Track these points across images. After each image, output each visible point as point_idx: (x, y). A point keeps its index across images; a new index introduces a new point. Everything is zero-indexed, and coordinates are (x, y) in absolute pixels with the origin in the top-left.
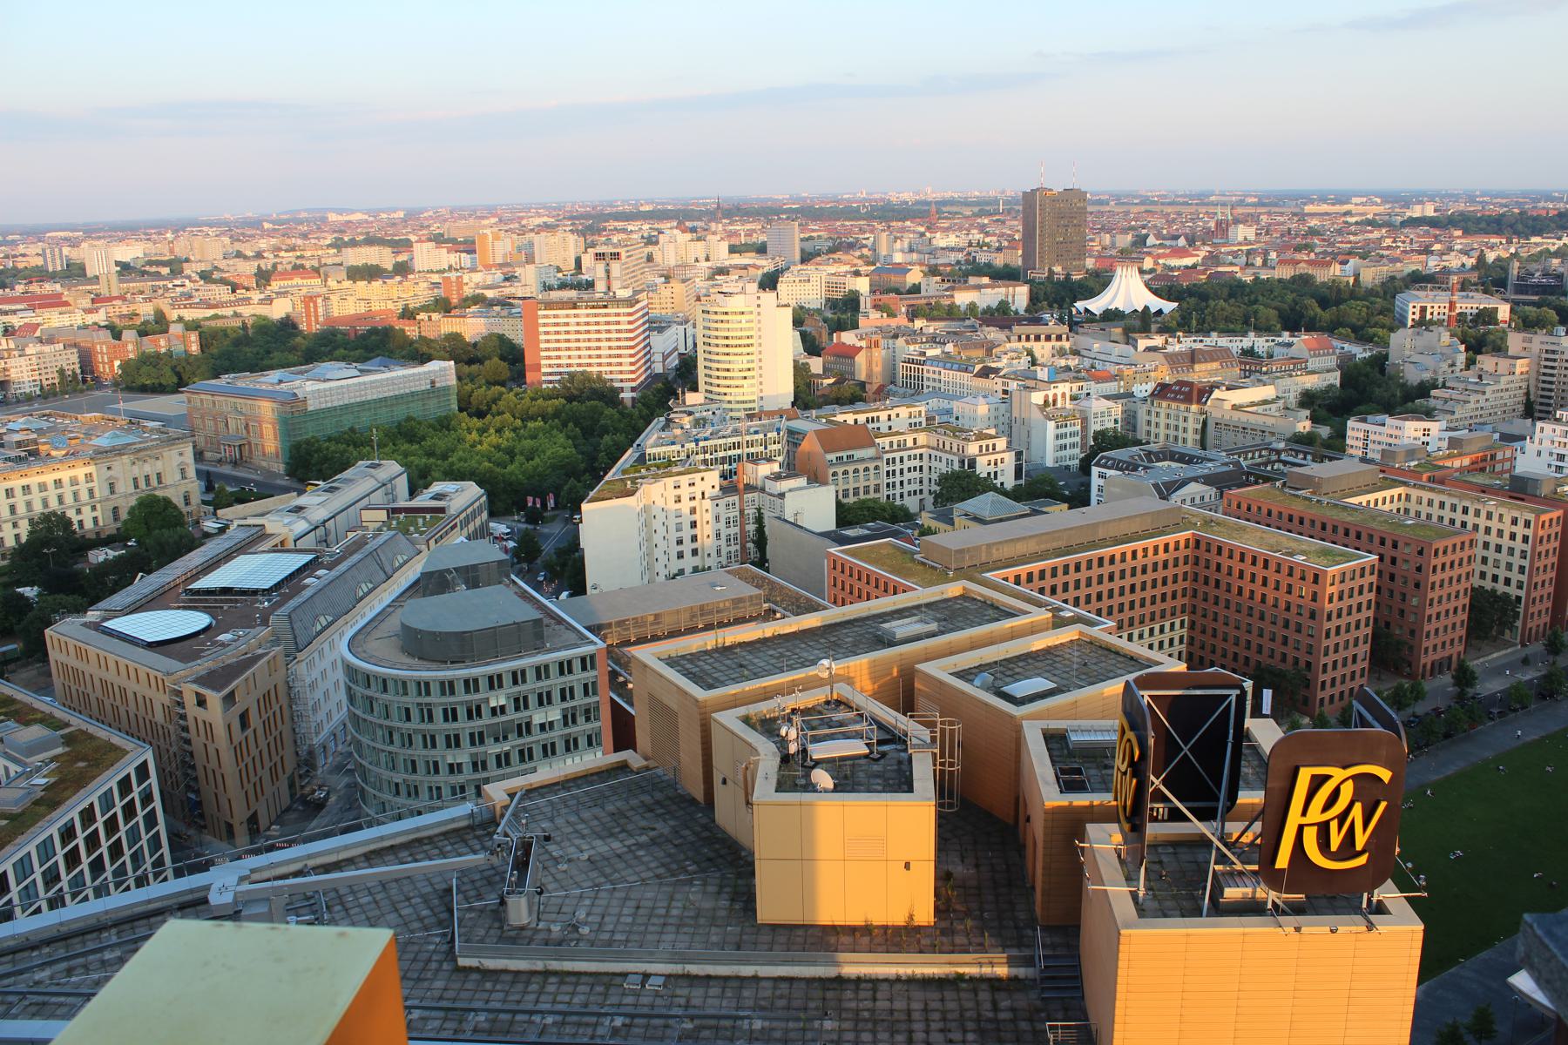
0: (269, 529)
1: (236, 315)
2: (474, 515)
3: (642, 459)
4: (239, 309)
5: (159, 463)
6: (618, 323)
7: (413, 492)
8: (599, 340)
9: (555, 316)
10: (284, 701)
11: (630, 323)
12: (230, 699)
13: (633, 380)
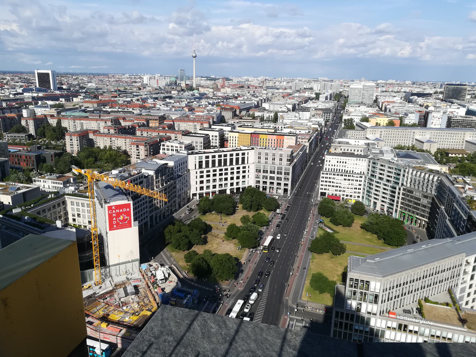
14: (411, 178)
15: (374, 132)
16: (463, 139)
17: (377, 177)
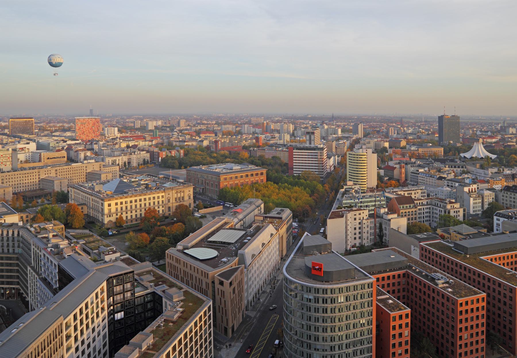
16: (39, 178)
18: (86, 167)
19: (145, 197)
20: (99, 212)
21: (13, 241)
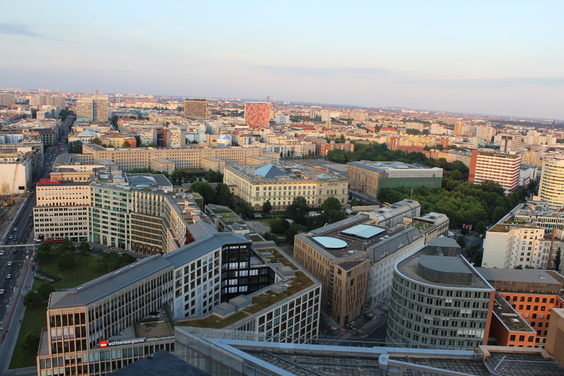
0: (371, 217)
1: (367, 140)
2: (444, 227)
3: (513, 219)
4: (369, 139)
5: (336, 187)
6: (508, 164)
7: (422, 214)
8: (499, 169)
9: (484, 158)
10: (366, 279)
11: (513, 165)
12: (349, 274)
13: (510, 187)
14: (138, 202)
15: (104, 155)
17: (103, 207)
18: (246, 151)
19: (295, 185)
20: (247, 194)
21: (159, 205)
